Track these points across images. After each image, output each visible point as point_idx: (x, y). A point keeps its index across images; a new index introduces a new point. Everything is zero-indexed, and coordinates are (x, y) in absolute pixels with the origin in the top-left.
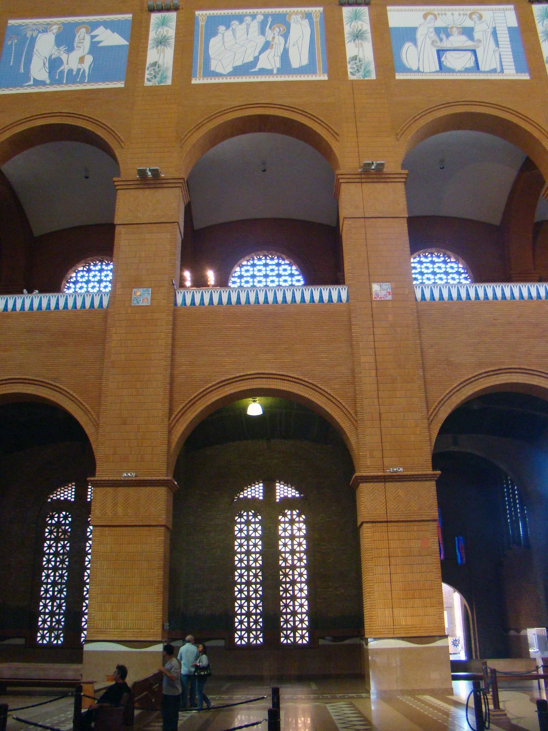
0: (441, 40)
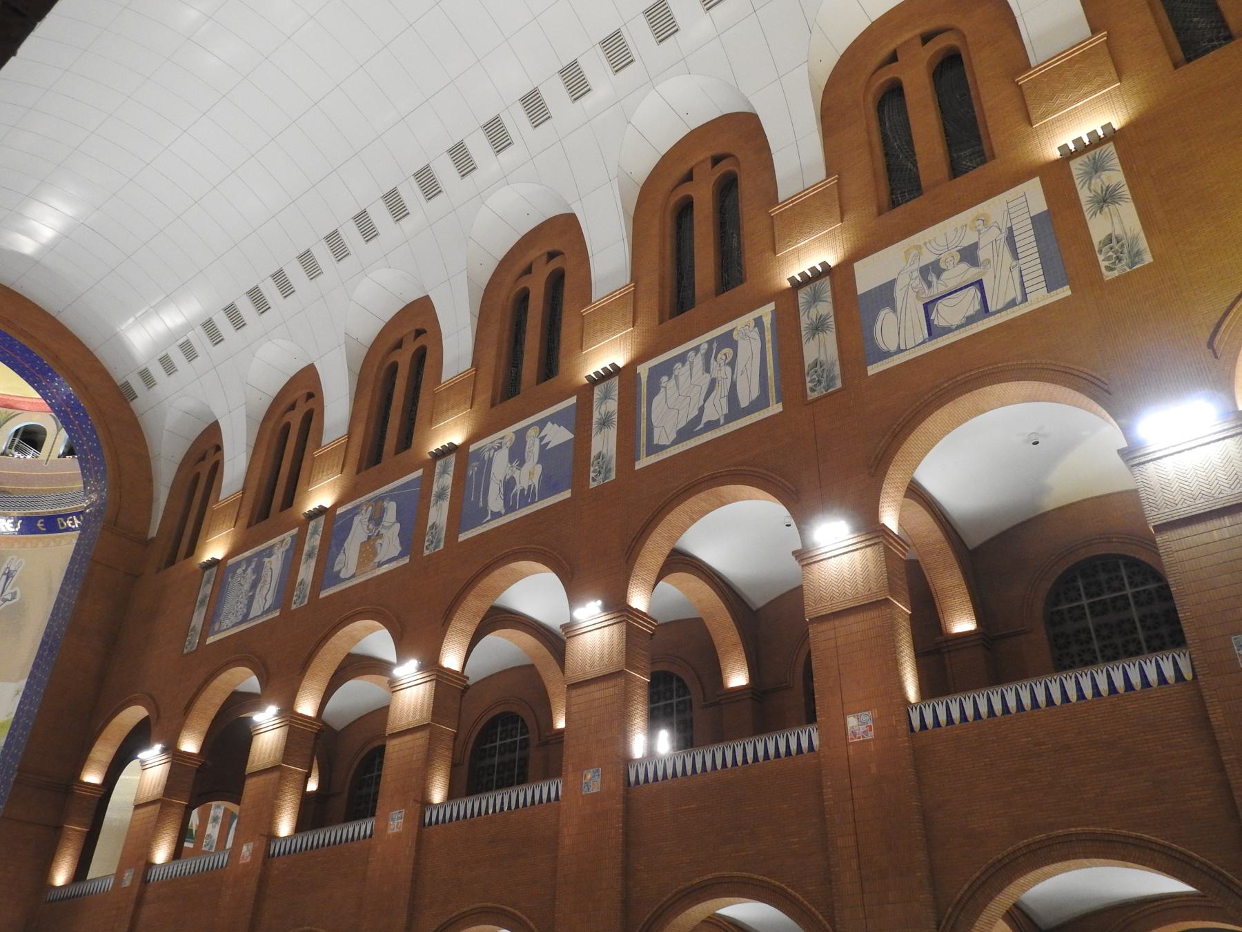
0: (930, 285)
